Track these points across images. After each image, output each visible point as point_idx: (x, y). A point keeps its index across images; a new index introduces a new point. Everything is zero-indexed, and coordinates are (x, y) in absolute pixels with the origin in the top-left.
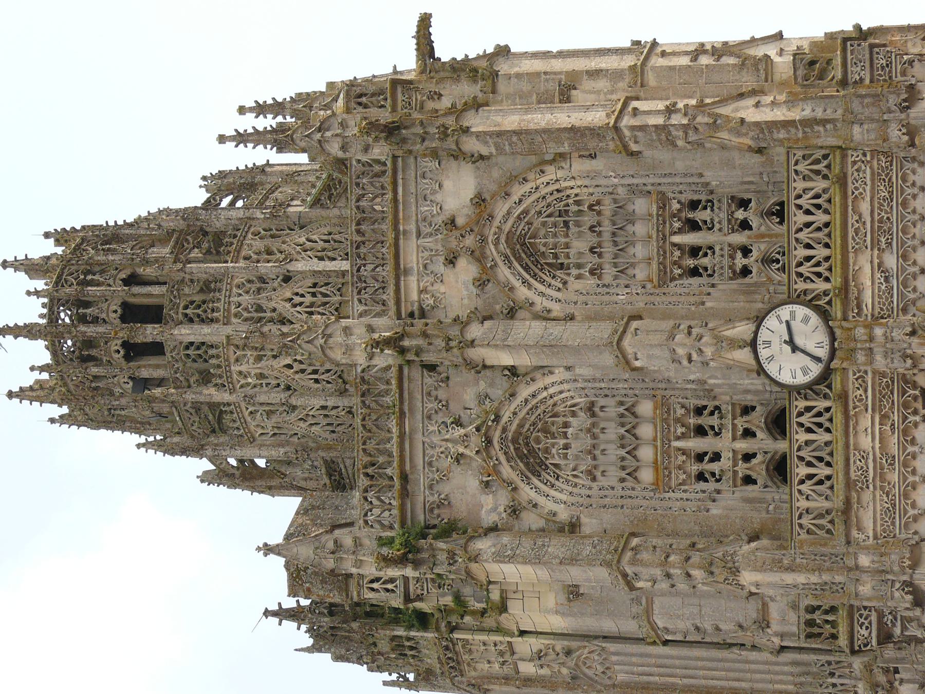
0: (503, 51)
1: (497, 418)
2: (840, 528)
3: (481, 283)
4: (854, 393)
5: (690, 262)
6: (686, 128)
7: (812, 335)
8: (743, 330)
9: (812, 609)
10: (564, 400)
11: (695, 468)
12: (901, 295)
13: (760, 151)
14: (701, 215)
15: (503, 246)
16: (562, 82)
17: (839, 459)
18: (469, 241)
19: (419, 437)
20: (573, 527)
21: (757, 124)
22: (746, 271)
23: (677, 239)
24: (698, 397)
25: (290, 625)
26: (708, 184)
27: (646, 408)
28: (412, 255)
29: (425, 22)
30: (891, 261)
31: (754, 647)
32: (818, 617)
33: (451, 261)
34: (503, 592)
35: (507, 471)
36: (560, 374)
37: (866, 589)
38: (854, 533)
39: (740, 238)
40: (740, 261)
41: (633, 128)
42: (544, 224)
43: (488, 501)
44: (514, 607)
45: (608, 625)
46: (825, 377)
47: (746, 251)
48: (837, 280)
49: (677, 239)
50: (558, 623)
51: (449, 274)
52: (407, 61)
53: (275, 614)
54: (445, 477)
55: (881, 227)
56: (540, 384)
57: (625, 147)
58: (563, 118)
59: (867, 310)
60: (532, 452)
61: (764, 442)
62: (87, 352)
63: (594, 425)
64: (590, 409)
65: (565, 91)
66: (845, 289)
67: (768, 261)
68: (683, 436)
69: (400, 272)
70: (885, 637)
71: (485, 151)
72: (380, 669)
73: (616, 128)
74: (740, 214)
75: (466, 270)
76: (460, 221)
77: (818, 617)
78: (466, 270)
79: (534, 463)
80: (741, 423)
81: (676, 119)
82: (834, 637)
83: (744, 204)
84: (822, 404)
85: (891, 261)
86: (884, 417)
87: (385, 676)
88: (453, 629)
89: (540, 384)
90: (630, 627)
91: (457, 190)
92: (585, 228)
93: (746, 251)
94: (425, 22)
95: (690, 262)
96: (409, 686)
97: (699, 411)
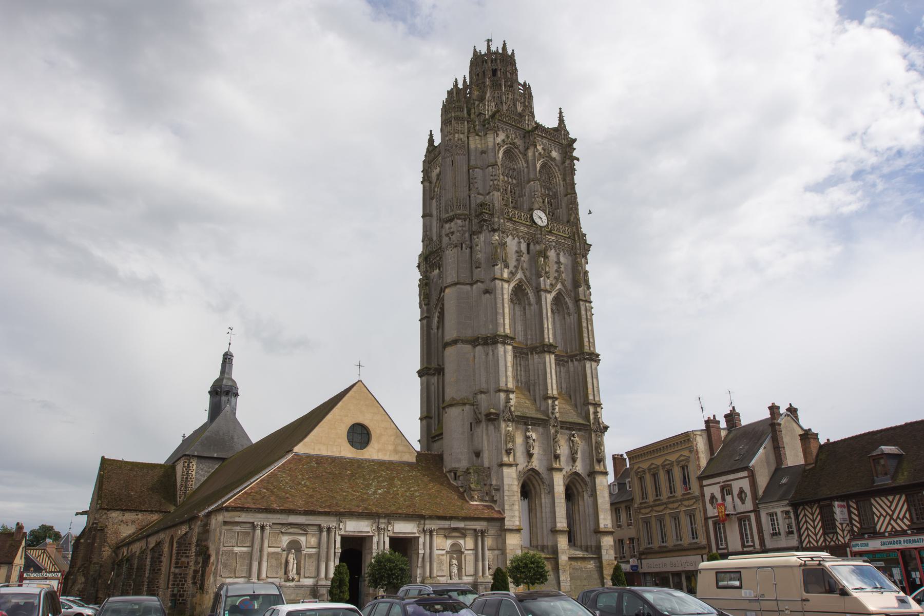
13: (568, 222)
27: (514, 181)
36: (525, 165)
44: (477, 137)
45: (472, 158)
46: (536, 224)
50: (472, 146)
61: (512, 205)
62: (484, 61)
70: (485, 221)
90: (472, 163)
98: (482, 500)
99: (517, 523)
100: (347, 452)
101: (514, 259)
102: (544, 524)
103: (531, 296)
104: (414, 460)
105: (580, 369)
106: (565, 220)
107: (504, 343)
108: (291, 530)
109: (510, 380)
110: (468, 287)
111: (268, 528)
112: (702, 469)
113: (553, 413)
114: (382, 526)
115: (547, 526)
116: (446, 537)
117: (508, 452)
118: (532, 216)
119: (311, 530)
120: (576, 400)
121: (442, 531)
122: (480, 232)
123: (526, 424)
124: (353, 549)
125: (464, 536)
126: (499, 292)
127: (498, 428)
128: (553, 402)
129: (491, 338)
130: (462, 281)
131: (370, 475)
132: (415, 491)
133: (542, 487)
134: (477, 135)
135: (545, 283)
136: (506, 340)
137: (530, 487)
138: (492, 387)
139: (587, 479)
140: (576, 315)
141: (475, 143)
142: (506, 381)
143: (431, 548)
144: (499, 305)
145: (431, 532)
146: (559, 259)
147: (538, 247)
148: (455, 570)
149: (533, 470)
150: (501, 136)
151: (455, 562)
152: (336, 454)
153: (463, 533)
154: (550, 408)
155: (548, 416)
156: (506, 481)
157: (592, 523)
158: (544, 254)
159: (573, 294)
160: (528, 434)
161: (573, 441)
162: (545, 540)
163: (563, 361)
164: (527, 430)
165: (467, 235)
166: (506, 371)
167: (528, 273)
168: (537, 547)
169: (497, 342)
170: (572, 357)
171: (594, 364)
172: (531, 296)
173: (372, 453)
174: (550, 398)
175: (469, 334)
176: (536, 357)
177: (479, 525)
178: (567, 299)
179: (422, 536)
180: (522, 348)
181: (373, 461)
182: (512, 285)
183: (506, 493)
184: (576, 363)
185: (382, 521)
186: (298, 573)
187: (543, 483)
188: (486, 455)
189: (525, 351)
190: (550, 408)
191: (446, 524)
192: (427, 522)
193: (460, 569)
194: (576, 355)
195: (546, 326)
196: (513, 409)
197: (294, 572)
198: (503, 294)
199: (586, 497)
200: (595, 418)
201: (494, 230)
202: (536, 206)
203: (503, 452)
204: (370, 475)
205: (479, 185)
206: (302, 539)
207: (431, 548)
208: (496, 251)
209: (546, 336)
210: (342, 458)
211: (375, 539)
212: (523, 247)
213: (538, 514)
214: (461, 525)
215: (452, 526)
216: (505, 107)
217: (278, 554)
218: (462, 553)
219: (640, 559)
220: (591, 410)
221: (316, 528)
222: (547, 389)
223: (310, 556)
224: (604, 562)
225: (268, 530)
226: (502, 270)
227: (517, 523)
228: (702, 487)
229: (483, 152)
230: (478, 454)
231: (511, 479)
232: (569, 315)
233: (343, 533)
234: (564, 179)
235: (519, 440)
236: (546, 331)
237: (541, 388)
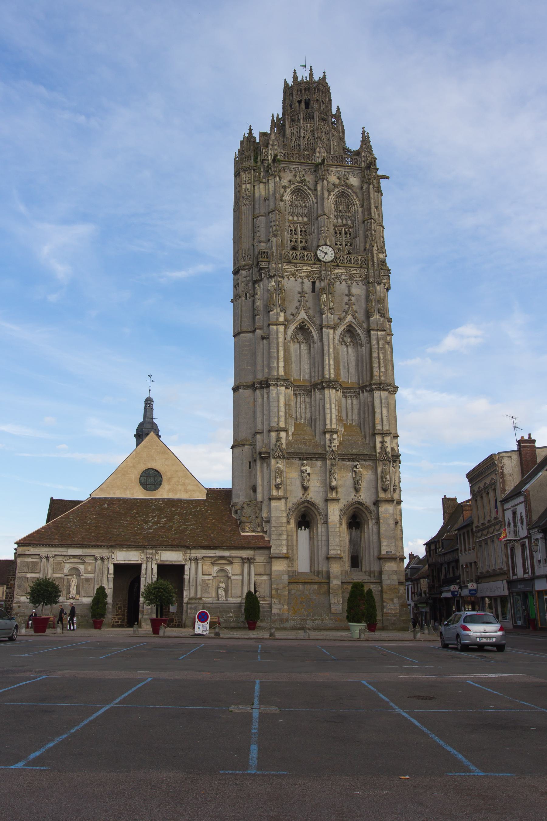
0: (382, 195)
1: (304, 185)
2: (287, 261)
3: (334, 184)
4: (316, 266)
5: (338, 232)
6: (371, 234)
7: (327, 258)
8: (328, 243)
9: (267, 253)
10: (307, 201)
11: (293, 229)
12: (336, 278)
13: (365, 250)
14: (348, 236)
15: (342, 190)
16: (378, 208)
17: (302, 262)
18: (343, 183)
19: (300, 167)
20: (282, 200)
21: (373, 250)
22: (336, 244)
23: (343, 229)
24: (309, 231)
25: (248, 131)
26: (356, 237)
27: (305, 219)
28: (340, 169)
29: (387, 178)
30: (343, 277)
31: (254, 239)
32: (266, 254)
33: (339, 178)
34: (265, 183)
35: (293, 186)
36: (315, 201)
37: (274, 265)
38: (285, 264)
39: (344, 244)
40: (339, 243)
41: (371, 222)
42: (345, 200)
43: (286, 181)
44: (261, 185)
45: (257, 206)
47: (340, 245)
48: (340, 264)
49: (343, 229)
50: (257, 195)
51: (335, 177)
52: (379, 173)
53: (250, 128)
54: (291, 171)
55: (351, 275)
56: (312, 196)
57: (366, 220)
58: (373, 207)
59: (333, 270)
60: (295, 192)
61: (300, 245)
63: (302, 207)
64: (305, 206)
65: (376, 208)
66: (338, 266)
67: (339, 249)
68: (300, 227)
69: (337, 166)
71: (364, 188)
72: (239, 152)
73: (371, 219)
74: (349, 244)
75: (337, 181)
76: (347, 181)
77: (266, 254)
78: (337, 181)
79: (293, 193)
80: (304, 240)
81: (373, 232)
82: (261, 257)
83: (351, 245)
84: (313, 259)
85: (343, 277)
86: (310, 272)
87: (237, 153)
88: (254, 170)
89: (312, 196)
90: (257, 212)
91: (354, 181)
92: (345, 209)
93: (340, 245)
94: (387, 178)
95: (338, 232)
96: (235, 158)
97: (305, 231)
98: (253, 531)
99: (285, 551)
100: (139, 493)
101: (296, 301)
102: (320, 552)
103: (315, 334)
104: (204, 497)
105: (370, 399)
106: (362, 248)
107: (276, 385)
108: (72, 560)
109: (282, 419)
110: (251, 335)
111: (51, 559)
112: (507, 492)
113: (330, 447)
114: (149, 556)
115: (322, 554)
116: (213, 564)
117: (278, 487)
118: (316, 254)
119: (89, 560)
120: (365, 432)
121: (209, 559)
122: (261, 280)
123: (301, 459)
124: (127, 574)
125: (231, 563)
126: (273, 337)
127: (269, 465)
128: (331, 436)
129: (264, 382)
130: (245, 330)
131: (153, 513)
132: (190, 525)
133: (318, 517)
134: (261, 182)
135: (328, 318)
136: (278, 382)
137: (306, 517)
138: (266, 427)
139: (372, 508)
140: (368, 345)
141: (260, 191)
142: (279, 421)
143: (196, 573)
144: (274, 350)
145: (197, 560)
146: (349, 291)
147: (323, 284)
148: (221, 592)
149: (307, 502)
150: (287, 177)
151: (223, 585)
152: (129, 496)
153: (230, 561)
154: (328, 443)
155: (326, 450)
156: (274, 514)
157: (376, 550)
158: (329, 290)
159: (365, 325)
160: (303, 468)
162: (320, 566)
163: (354, 393)
164: (302, 465)
165: (251, 284)
166: (278, 412)
167: (311, 312)
168: (314, 572)
169: (268, 386)
170: (362, 388)
171: (385, 394)
172: (315, 334)
173: (164, 493)
174: (328, 432)
175: (249, 379)
176: (317, 393)
177: (245, 554)
178: (359, 331)
179: (188, 563)
180: (306, 386)
181: (163, 500)
182: (292, 328)
183: (273, 524)
184: (366, 394)
185: (150, 551)
186: (78, 593)
187: (319, 513)
188: (259, 490)
189: (309, 388)
190: (328, 443)
191: (211, 553)
192: (193, 551)
193: (227, 591)
194: (365, 386)
195: (327, 362)
196: (284, 446)
197: (74, 592)
198: (277, 338)
199: (370, 525)
200: (381, 448)
201: (271, 277)
202: (322, 242)
203: (273, 487)
204: (153, 513)
205: (262, 234)
206: (82, 567)
207: (196, 573)
208: (272, 297)
209: (326, 372)
210: (134, 499)
211: (143, 567)
212: (308, 285)
213: (315, 542)
214: (226, 553)
215: (217, 555)
216: (302, 142)
217: (61, 578)
218: (228, 577)
219: (477, 582)
220: (378, 439)
221: (92, 558)
222: (325, 425)
223: (88, 580)
224: (384, 587)
225: (51, 560)
226: (278, 315)
227: (285, 551)
228: (504, 511)
229: (266, 199)
230: (255, 490)
231: (279, 511)
232: (361, 345)
233: (115, 562)
234: (363, 206)
235: (293, 476)
236: (327, 368)
237: (322, 423)
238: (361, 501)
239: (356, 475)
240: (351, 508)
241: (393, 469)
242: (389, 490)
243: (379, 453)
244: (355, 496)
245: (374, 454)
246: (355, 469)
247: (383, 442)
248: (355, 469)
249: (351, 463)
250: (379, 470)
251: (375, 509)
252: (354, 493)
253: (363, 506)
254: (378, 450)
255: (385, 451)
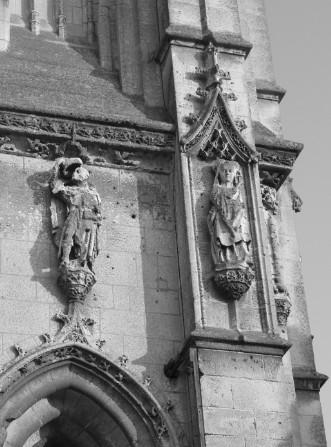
161: (62, 201)
220: (183, 64)
238: (93, 348)
239: (65, 216)
240: (37, 386)
241: (266, 214)
242: (250, 295)
243: (189, 121)
244: (61, 322)
245: (167, 126)
246: (59, 186)
247: (207, 78)
248: (59, 186)
249: (40, 164)
250: (193, 195)
251: (174, 398)
252: (48, 304)
253: (105, 383)
254: (184, 109)
255: (224, 114)
